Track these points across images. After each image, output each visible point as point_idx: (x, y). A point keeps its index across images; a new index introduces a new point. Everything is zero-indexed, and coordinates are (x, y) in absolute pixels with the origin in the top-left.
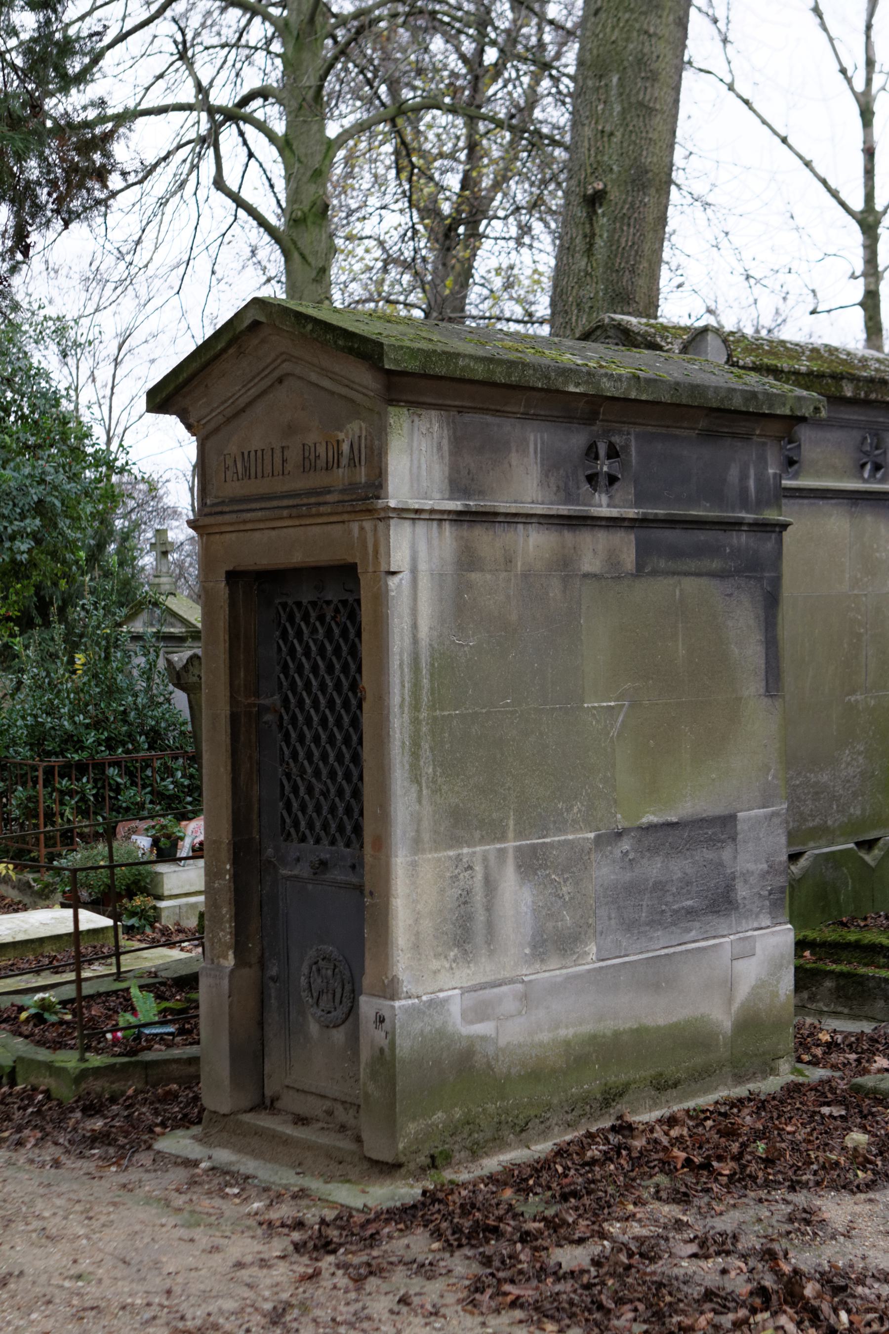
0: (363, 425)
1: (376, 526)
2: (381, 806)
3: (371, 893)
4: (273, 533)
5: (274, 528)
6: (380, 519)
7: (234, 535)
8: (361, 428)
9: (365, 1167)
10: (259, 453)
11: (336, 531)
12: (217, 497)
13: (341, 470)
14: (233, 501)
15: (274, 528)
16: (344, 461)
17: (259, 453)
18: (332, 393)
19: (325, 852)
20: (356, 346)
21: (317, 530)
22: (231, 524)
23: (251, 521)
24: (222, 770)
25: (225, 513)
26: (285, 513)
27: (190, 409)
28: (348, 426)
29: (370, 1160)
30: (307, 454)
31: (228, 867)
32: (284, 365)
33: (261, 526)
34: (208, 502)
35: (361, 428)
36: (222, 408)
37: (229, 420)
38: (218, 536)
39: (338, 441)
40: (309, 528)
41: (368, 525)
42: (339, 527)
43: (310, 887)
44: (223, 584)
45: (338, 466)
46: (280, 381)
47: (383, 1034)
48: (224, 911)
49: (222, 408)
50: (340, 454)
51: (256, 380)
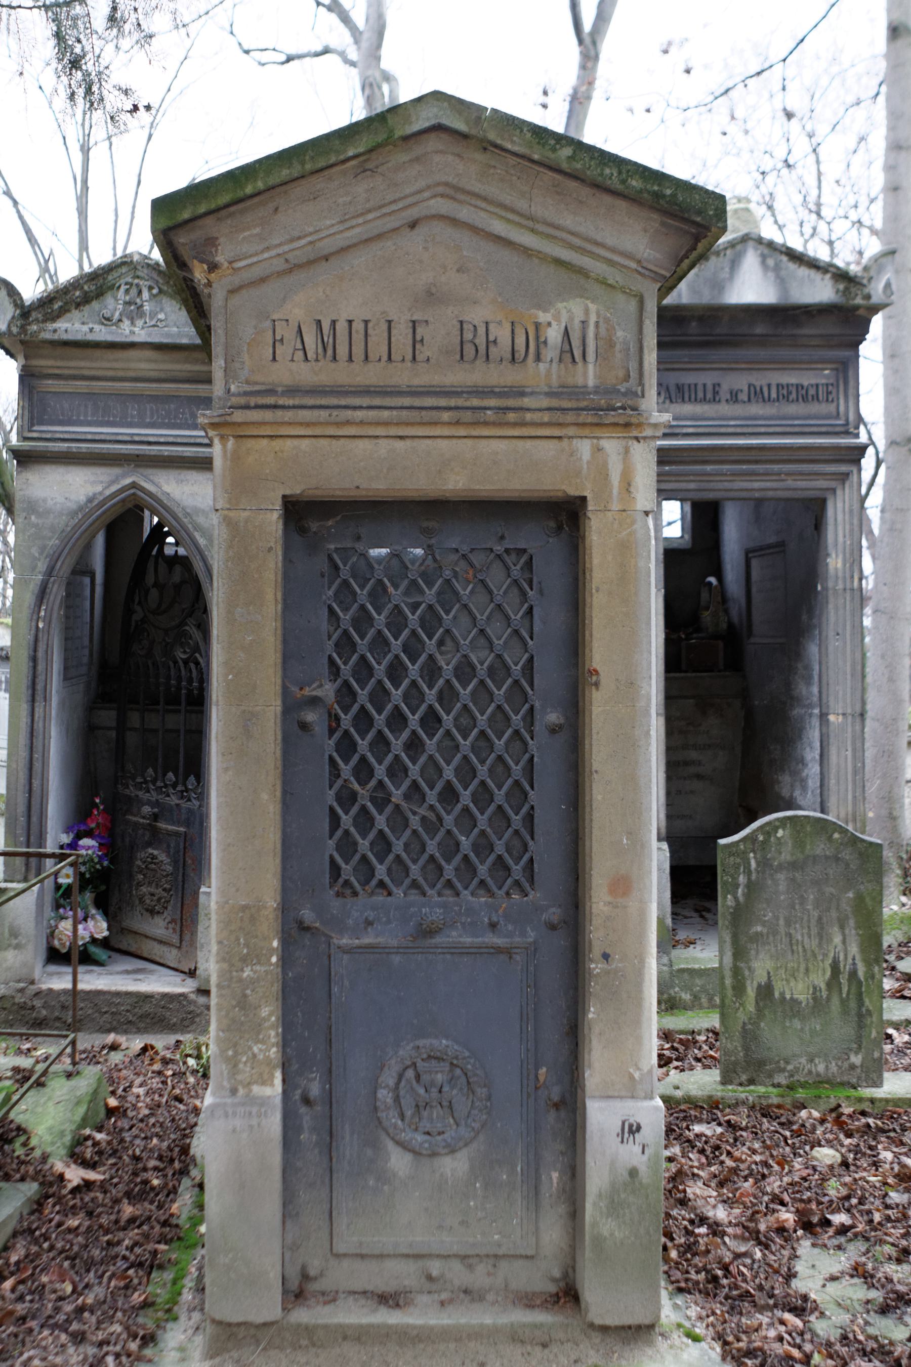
0: (593, 307)
1: (627, 451)
2: (630, 833)
3: (606, 957)
4: (399, 445)
5: (401, 438)
6: (637, 439)
7: (306, 442)
8: (587, 311)
9: (597, 1341)
10: (358, 326)
11: (546, 450)
12: (247, 382)
13: (542, 366)
14: (292, 391)
15: (401, 438)
16: (550, 353)
17: (358, 326)
18: (526, 251)
19: (433, 907)
20: (668, 192)
21: (501, 445)
22: (308, 425)
23: (362, 423)
24: (265, 796)
25: (283, 407)
26: (446, 416)
27: (222, 240)
28: (560, 305)
29: (605, 1329)
30: (468, 336)
31: (275, 944)
32: (432, 202)
33: (380, 431)
34: (233, 388)
35: (587, 311)
36: (286, 248)
37: (292, 269)
38: (265, 442)
39: (537, 326)
40: (484, 442)
41: (611, 446)
42: (552, 445)
43: (396, 959)
44: (275, 515)
45: (538, 358)
46: (413, 225)
47: (637, 1149)
48: (265, 1012)
49: (286, 248)
50: (542, 343)
51: (370, 216)
